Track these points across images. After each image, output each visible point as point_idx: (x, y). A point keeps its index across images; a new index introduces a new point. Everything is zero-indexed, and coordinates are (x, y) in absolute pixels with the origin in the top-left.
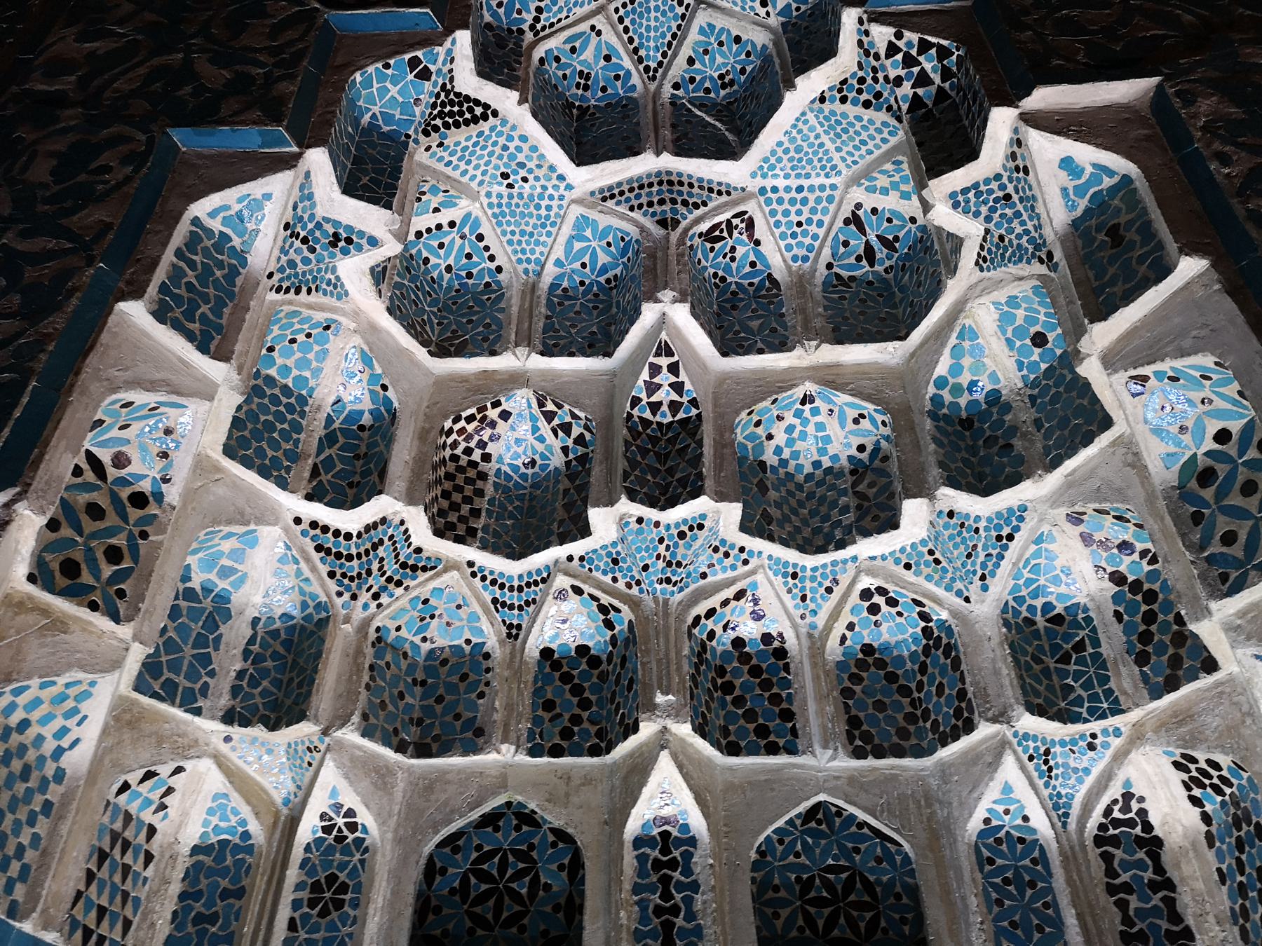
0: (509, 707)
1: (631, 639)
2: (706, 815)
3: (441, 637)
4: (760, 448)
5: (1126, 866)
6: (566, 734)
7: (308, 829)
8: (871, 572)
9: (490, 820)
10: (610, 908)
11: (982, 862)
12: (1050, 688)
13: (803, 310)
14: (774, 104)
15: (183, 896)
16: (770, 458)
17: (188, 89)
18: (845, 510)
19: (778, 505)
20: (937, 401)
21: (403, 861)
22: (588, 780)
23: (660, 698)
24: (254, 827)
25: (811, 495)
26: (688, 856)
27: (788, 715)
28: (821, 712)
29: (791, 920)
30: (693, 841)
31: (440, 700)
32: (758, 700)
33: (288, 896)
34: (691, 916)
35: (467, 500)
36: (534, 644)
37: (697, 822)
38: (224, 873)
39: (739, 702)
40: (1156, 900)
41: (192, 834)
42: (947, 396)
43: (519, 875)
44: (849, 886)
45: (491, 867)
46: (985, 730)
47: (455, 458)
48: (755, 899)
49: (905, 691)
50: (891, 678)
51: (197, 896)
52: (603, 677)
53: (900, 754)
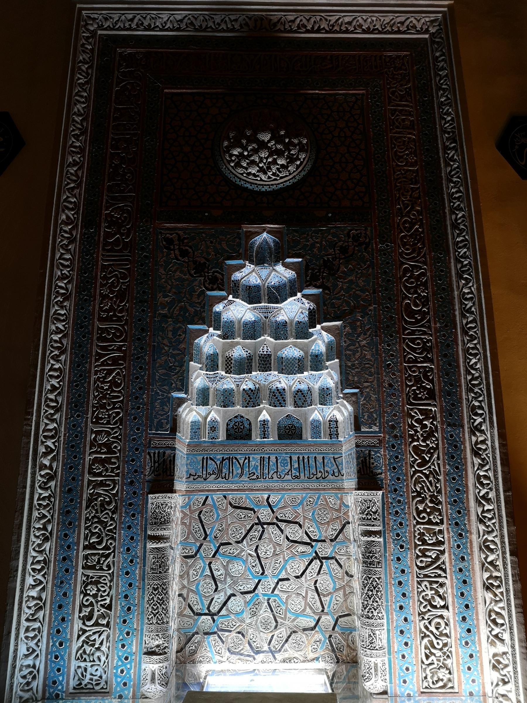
0: (238, 399)
1: (258, 390)
2: (270, 416)
3: (225, 386)
4: (282, 355)
5: (332, 425)
6: (248, 404)
7: (209, 419)
8: (299, 379)
9: (236, 417)
10: (256, 431)
11: (312, 424)
12: (324, 400)
13: (291, 330)
14: (286, 299)
15: (191, 429)
16: (284, 356)
17: (187, 314)
18: (296, 367)
19: (285, 366)
20: (312, 353)
21: (224, 424)
22: (252, 411)
23: (264, 401)
24: (200, 419)
25: (291, 362)
26: (268, 423)
27: (284, 401)
28: (290, 400)
29: (283, 432)
30: (268, 421)
31: (226, 398)
32: (280, 398)
33: (207, 429)
34: (268, 432)
35: (230, 365)
36: (241, 389)
37: (269, 419)
38: (196, 426)
39: (277, 398)
40: (335, 429)
41: (190, 420)
42: (314, 351)
43: (241, 425)
44: (292, 427)
45: (237, 424)
46: (313, 406)
47: (227, 357)
48: (278, 429)
49: (304, 396)
50: (302, 394)
51: (193, 429)
52: (254, 393)
53: (302, 407)
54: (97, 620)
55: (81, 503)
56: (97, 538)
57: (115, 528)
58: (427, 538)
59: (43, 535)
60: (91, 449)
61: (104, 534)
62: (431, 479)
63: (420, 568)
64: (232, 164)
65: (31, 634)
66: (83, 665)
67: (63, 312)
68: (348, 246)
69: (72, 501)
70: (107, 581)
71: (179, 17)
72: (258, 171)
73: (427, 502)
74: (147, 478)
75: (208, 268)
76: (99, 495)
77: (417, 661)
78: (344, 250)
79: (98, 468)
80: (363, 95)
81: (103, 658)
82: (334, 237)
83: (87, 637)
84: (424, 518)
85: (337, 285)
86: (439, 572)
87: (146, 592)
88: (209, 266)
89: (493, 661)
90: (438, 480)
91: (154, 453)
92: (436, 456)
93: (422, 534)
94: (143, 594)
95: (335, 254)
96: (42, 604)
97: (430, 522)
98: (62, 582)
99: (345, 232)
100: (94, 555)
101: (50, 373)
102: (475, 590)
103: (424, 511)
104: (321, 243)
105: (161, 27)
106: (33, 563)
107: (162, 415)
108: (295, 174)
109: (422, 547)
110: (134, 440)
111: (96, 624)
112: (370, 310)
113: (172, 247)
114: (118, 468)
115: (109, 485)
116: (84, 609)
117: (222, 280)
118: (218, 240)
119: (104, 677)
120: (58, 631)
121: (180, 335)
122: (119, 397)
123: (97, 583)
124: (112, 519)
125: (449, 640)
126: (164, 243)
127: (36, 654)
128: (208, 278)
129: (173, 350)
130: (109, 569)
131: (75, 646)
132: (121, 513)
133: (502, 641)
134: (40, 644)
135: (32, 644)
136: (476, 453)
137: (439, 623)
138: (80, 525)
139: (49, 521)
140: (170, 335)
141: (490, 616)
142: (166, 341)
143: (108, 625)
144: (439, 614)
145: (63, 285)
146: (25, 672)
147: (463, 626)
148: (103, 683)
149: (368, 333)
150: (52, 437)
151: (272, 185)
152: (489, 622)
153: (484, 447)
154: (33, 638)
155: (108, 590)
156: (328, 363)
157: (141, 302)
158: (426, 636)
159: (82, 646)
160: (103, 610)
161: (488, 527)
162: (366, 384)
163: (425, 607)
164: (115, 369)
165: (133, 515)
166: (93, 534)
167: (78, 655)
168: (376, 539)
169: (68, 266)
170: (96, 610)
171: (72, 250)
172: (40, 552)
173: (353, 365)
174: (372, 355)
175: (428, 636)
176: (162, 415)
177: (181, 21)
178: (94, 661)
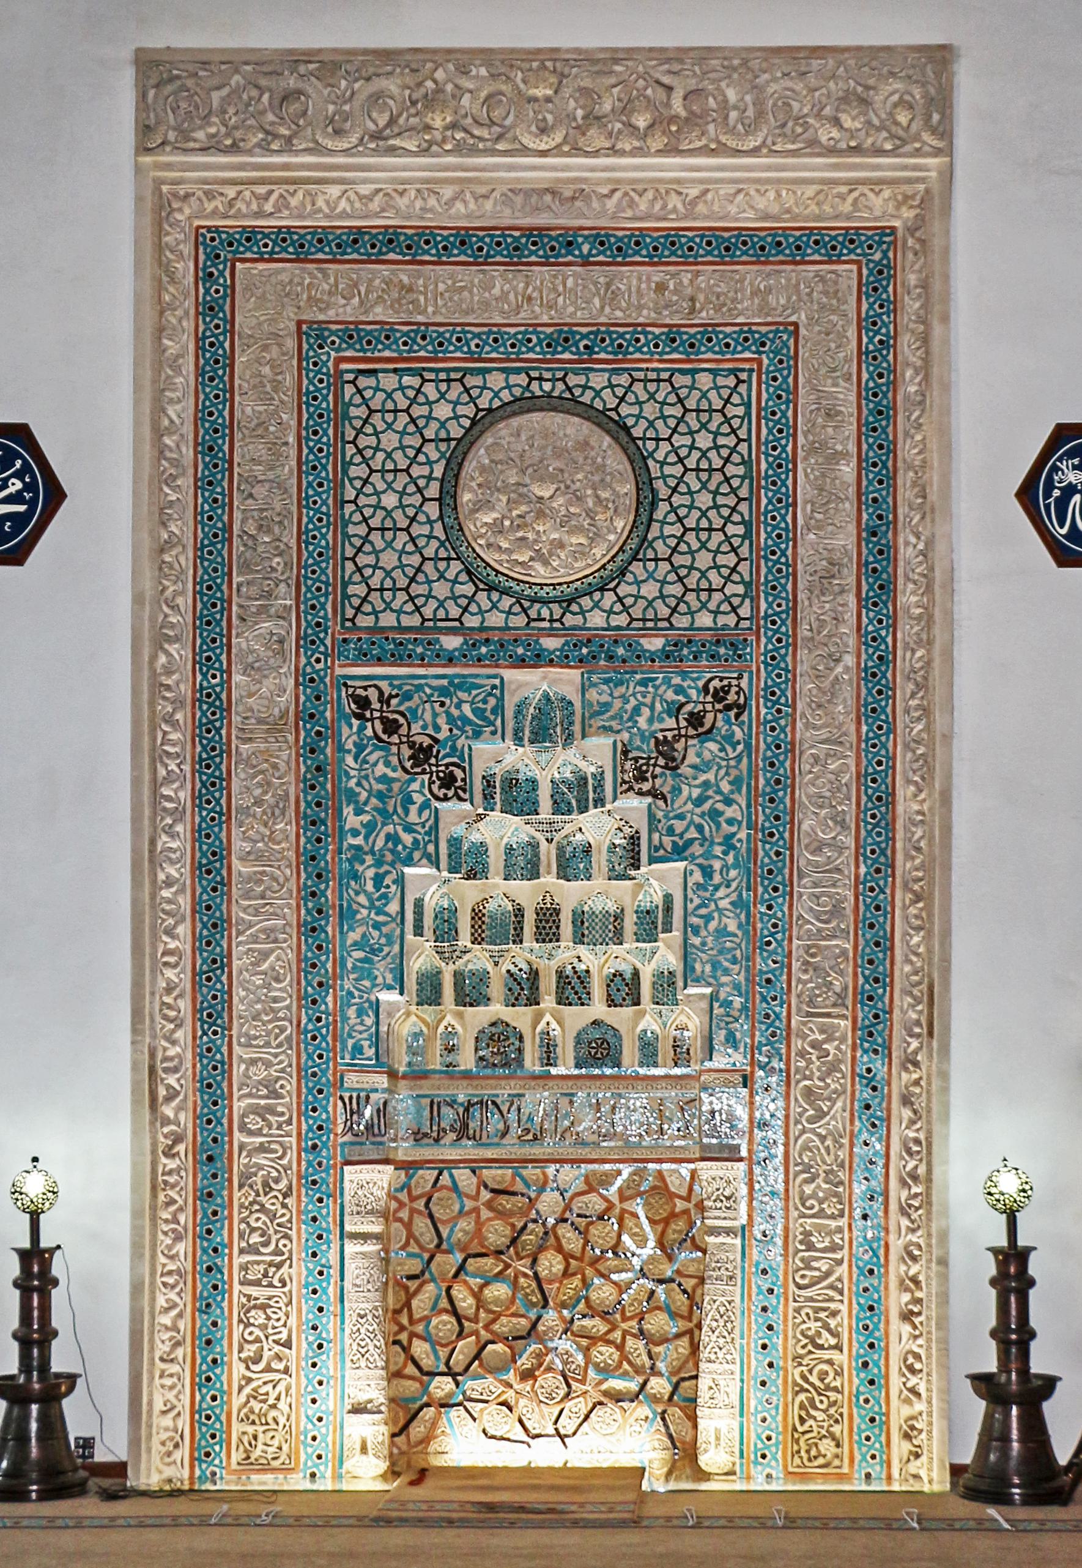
17: (400, 847)
54: (268, 1364)
55: (230, 1180)
56: (262, 1236)
57: (290, 1221)
58: (813, 1239)
59: (174, 1231)
60: (239, 1090)
61: (271, 1231)
62: (828, 1142)
63: (800, 1287)
64: (482, 542)
65: (168, 1382)
66: (251, 1429)
67: (174, 845)
68: (705, 711)
69: (215, 1176)
70: (281, 1305)
71: (365, 189)
72: (532, 559)
73: (820, 1181)
74: (340, 1140)
75: (436, 757)
76: (261, 1168)
77: (785, 1427)
78: (695, 720)
79: (254, 1122)
80: (751, 370)
81: (282, 1421)
82: (677, 693)
83: (255, 1390)
84: (812, 1207)
85: (680, 791)
86: (831, 1293)
87: (347, 1321)
88: (438, 752)
89: (905, 1427)
90: (841, 1146)
91: (351, 1098)
92: (839, 1104)
93: (807, 1234)
94: (343, 1323)
95: (679, 729)
96: (179, 1338)
97: (821, 1214)
98: (208, 1305)
99: (701, 683)
100: (258, 1263)
101: (165, 959)
102: (887, 1322)
103: (814, 1196)
104: (652, 708)
105: (327, 211)
106: (162, 1275)
107: (361, 1033)
108: (605, 560)
109: (806, 1254)
110: (314, 1075)
111: (268, 1369)
112: (740, 840)
113: (368, 714)
114: (289, 1122)
115: (276, 1151)
116: (247, 1346)
117: (464, 780)
118: (455, 700)
119: (285, 1447)
120: (208, 1379)
121: (388, 887)
122: (285, 999)
123: (264, 1307)
124: (284, 1206)
125: (840, 1396)
126: (353, 706)
127: (175, 1412)
128: (438, 777)
129: (377, 914)
130: (284, 1285)
131: (237, 1401)
132: (299, 1196)
133: (918, 1395)
134: (181, 1397)
135: (171, 1396)
136: (906, 1101)
137: (827, 1373)
138: (230, 1217)
139: (181, 1209)
140: (370, 887)
141: (905, 1360)
142: (362, 899)
143: (286, 1371)
144: (826, 1357)
145: (172, 794)
146: (164, 1436)
147: (862, 1375)
148: (283, 1457)
149: (734, 885)
150: (175, 1070)
151: (560, 584)
152: (904, 1370)
153: (917, 1090)
154: (172, 1388)
155: (284, 1318)
156: (661, 936)
157: (313, 823)
158: (803, 1390)
159: (248, 1402)
160: (277, 1348)
161: (913, 1222)
162: (724, 979)
163: (803, 1347)
164: (272, 951)
165: (320, 1200)
166: (253, 1230)
167: (242, 1414)
168: (728, 1240)
169: (178, 755)
170: (266, 1348)
171: (181, 722)
172: (172, 1258)
173: (704, 944)
174: (740, 926)
175: (807, 1391)
176: (361, 1033)
177: (370, 198)
178: (267, 1424)
